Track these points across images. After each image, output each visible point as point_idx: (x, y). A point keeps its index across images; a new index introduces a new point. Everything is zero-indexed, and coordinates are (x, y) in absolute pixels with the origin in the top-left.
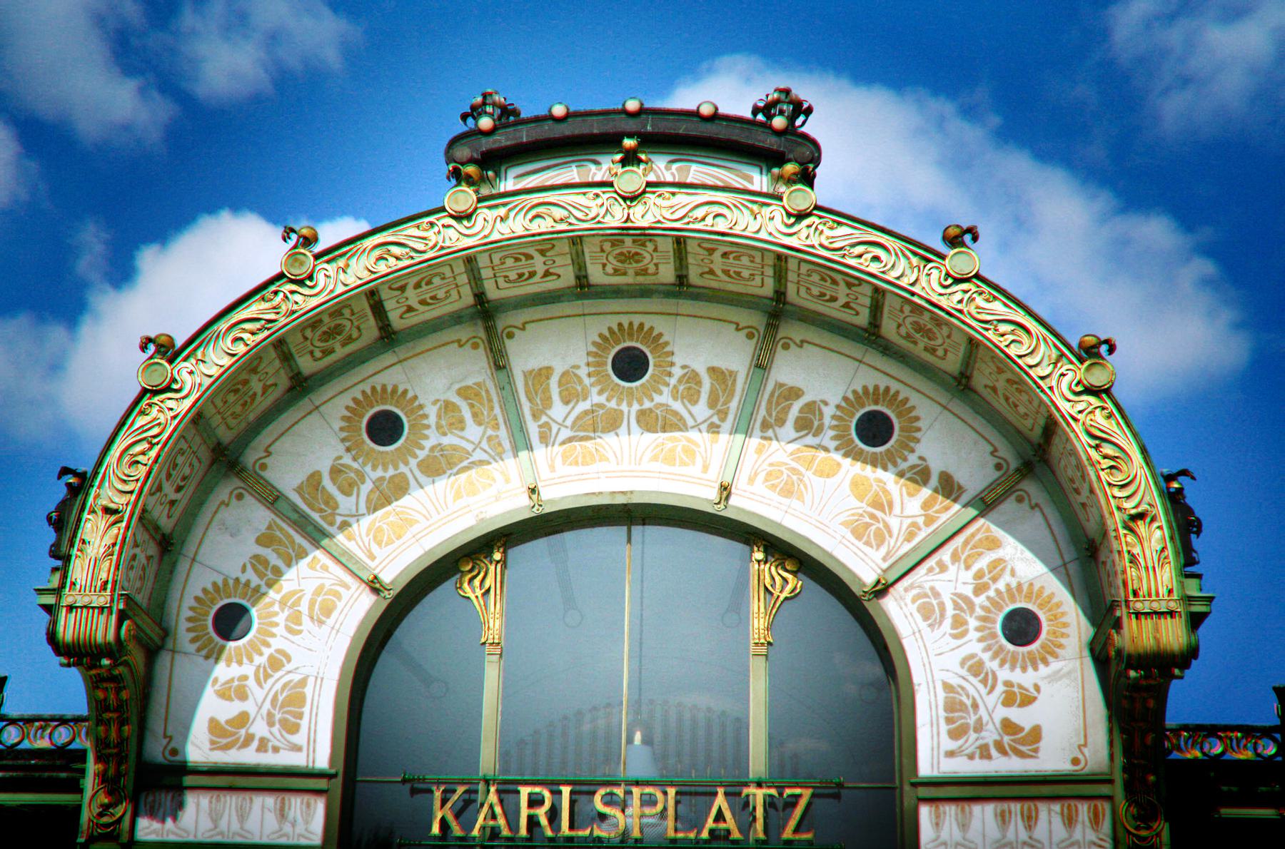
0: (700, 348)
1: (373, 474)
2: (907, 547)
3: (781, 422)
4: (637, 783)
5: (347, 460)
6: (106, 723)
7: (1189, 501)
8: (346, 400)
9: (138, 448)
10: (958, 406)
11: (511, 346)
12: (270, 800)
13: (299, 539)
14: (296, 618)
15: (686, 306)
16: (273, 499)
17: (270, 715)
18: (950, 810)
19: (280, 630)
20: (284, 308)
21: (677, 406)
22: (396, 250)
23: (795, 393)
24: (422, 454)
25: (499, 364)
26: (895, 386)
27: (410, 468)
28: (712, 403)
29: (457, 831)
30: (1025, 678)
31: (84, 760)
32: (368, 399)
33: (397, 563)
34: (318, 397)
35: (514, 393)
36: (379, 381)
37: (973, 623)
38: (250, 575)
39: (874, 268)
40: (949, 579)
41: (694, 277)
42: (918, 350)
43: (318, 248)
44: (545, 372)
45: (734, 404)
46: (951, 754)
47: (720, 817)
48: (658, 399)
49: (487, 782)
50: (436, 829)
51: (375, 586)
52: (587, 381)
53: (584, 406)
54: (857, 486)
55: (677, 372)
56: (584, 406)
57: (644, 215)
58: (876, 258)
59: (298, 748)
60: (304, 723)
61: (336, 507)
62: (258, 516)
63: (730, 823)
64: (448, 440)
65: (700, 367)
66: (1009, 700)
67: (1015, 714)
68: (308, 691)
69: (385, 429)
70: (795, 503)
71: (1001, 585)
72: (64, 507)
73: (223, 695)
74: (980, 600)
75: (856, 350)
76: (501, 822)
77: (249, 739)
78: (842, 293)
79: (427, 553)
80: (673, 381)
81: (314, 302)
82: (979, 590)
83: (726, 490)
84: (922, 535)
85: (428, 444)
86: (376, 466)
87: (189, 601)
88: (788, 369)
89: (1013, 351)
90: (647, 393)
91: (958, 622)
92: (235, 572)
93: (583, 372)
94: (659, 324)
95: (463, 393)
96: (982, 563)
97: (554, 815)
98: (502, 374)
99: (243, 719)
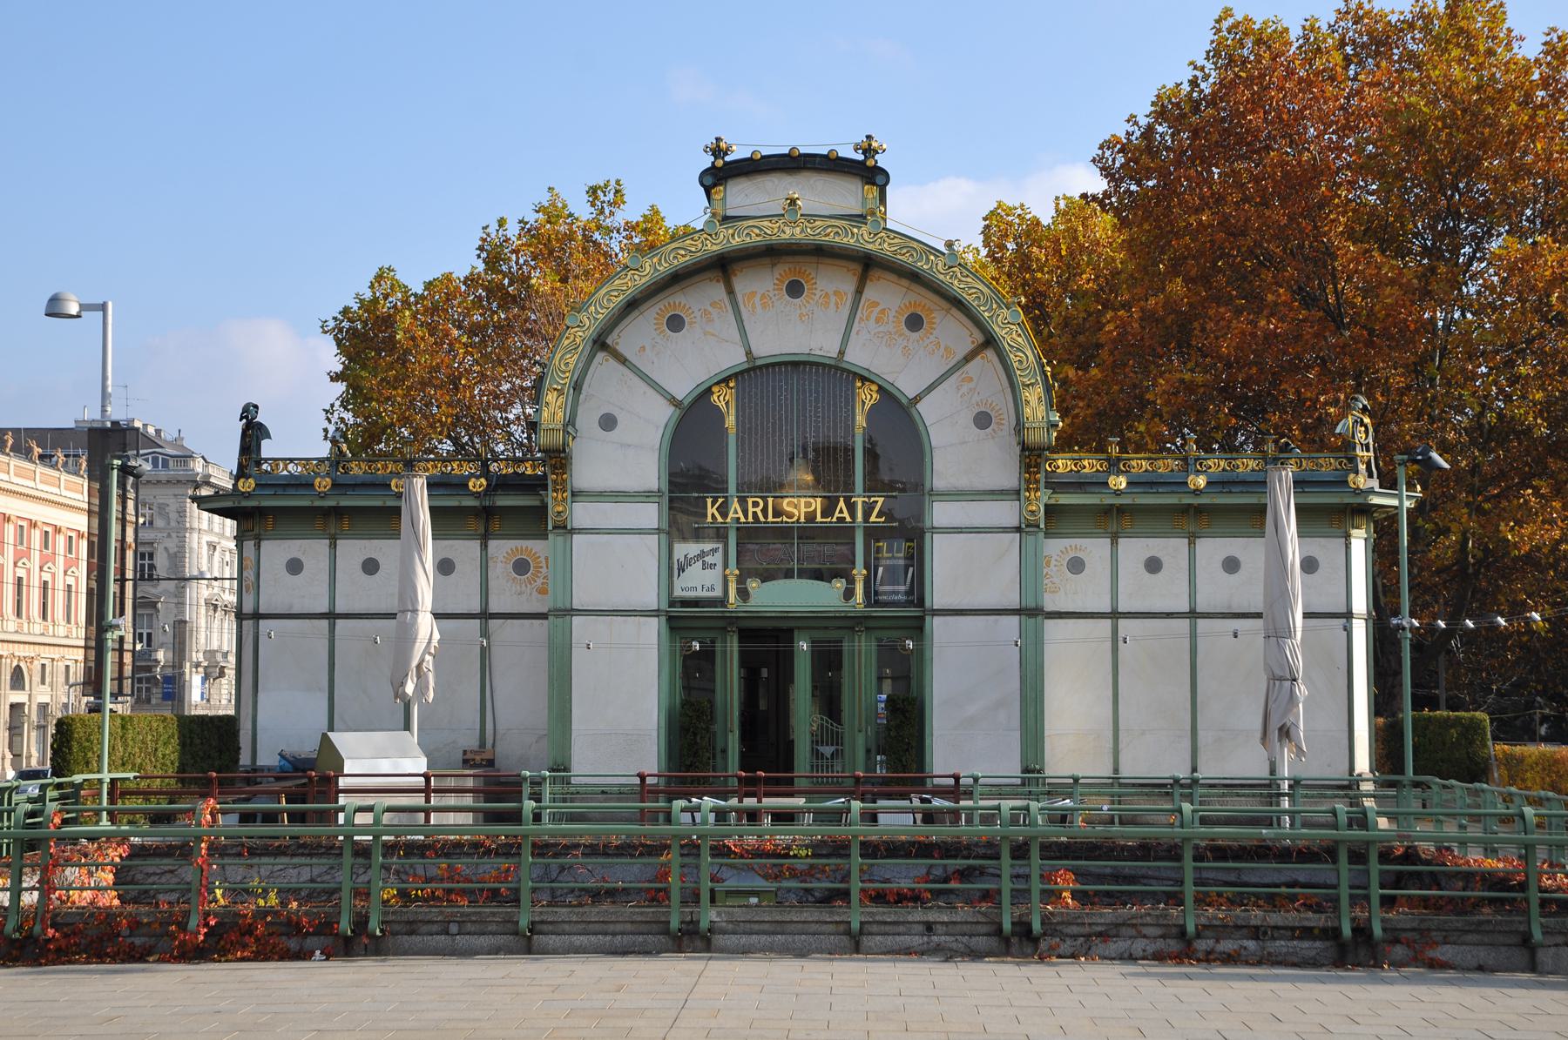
8: (656, 309)
10: (954, 311)
16: (623, 361)
33: (683, 389)
47: (841, 511)
50: (709, 519)
55: (818, 293)
63: (846, 514)
65: (831, 293)
76: (741, 515)
96: (964, 389)
97: (765, 511)
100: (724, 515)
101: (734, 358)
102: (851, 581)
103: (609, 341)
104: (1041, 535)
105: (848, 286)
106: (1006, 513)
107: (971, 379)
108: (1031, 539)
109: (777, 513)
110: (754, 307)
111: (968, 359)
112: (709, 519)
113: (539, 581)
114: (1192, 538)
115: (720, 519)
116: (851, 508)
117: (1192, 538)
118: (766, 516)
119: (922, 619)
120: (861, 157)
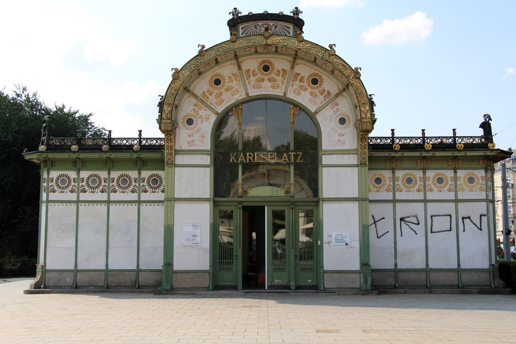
0: (280, 63)
1: (215, 91)
2: (321, 105)
3: (296, 80)
4: (269, 152)
5: (210, 89)
6: (168, 143)
7: (373, 100)
9: (173, 91)
10: (331, 77)
11: (242, 65)
12: (200, 156)
13: (202, 105)
14: (202, 121)
15: (277, 56)
16: (196, 96)
17: (199, 140)
18: (328, 156)
19: (199, 123)
20: (199, 62)
21: (275, 77)
22: (221, 50)
23: (299, 74)
24: (225, 87)
25: (240, 68)
26: (319, 73)
27: (223, 91)
28: (283, 76)
29: (235, 161)
30: (343, 132)
31: (164, 149)
32: (214, 76)
33: (220, 109)
34: (204, 76)
35: (243, 75)
36: (216, 72)
37: (333, 120)
38: (193, 113)
39: (315, 53)
41: (279, 50)
43: (205, 49)
44: (249, 70)
45: (287, 77)
46: (328, 146)
48: (272, 75)
49: (240, 152)
50: (231, 161)
51: (217, 113)
52: (257, 72)
53: (257, 77)
54: (311, 93)
55: (275, 70)
56: (257, 77)
57: (269, 41)
58: (315, 51)
59: (204, 146)
60: (205, 141)
61: (208, 98)
62: (193, 100)
63: (287, 159)
64: (230, 84)
66: (339, 135)
67: (340, 138)
68: (205, 135)
69: (217, 82)
70: (299, 97)
71: (338, 113)
72: (160, 103)
73: (190, 136)
74: (335, 116)
75: (311, 65)
76: (244, 159)
77: (195, 144)
78: (309, 56)
79: (227, 107)
80: (275, 72)
81: (205, 60)
82: (335, 114)
83: (285, 94)
84: (323, 103)
85: (226, 85)
86: (216, 90)
87: (181, 118)
88: (298, 69)
89: (341, 70)
90: (269, 74)
91: (330, 120)
92: (190, 112)
93: (257, 70)
94: (271, 60)
95: (233, 74)
98: (240, 71)
100: (237, 160)
101: (241, 96)
103: (191, 89)
104: (367, 168)
106: (353, 159)
107: (337, 105)
108: (363, 168)
110: (250, 76)
111: (337, 96)
112: (231, 161)
113: (162, 187)
114: (424, 170)
115: (235, 161)
116: (289, 156)
117: (424, 170)
118: (254, 160)
119: (318, 202)
120: (292, 15)
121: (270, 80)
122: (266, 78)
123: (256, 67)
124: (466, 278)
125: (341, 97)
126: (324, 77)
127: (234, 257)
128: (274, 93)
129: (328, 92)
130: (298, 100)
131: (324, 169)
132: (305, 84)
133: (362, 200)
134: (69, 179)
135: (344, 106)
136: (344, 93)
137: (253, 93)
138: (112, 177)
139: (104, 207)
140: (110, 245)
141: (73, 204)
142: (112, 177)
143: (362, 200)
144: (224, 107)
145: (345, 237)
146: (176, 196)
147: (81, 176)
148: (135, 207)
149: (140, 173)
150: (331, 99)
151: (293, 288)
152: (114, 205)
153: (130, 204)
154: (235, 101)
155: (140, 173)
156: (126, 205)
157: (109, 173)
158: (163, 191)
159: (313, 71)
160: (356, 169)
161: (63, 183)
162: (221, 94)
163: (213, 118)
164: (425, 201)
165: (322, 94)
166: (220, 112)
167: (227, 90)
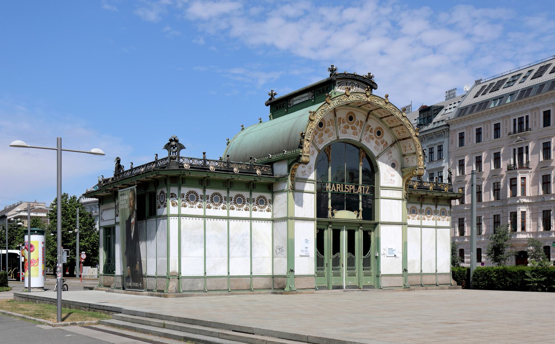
11: (337, 113)
15: (358, 110)
23: (370, 126)
25: (335, 116)
27: (323, 132)
33: (321, 147)
40: (385, 157)
42: (387, 123)
54: (376, 142)
64: (328, 128)
66: (391, 176)
67: (392, 178)
75: (378, 120)
88: (370, 122)
95: (331, 120)
99: (305, 171)
101: (333, 138)
102: (359, 211)
105: (363, 119)
107: (391, 153)
109: (344, 190)
111: (391, 146)
121: (352, 128)
122: (350, 126)
123: (345, 116)
124: (441, 280)
125: (393, 147)
126: (385, 131)
127: (325, 265)
128: (354, 139)
129: (386, 142)
130: (368, 146)
131: (382, 200)
132: (373, 134)
133: (403, 224)
134: (197, 195)
135: (395, 153)
136: (395, 144)
137: (342, 137)
138: (230, 196)
139: (225, 222)
140: (231, 256)
141: (201, 219)
142: (230, 196)
143: (403, 224)
144: (323, 146)
145: (394, 250)
146: (296, 216)
147: (207, 193)
148: (247, 223)
149: (251, 194)
150: (388, 148)
151: (362, 287)
152: (232, 220)
153: (244, 221)
154: (330, 141)
155: (251, 194)
156: (241, 221)
157: (228, 193)
158: (268, 211)
159: (379, 125)
160: (401, 201)
161: (192, 198)
162: (322, 135)
163: (316, 154)
164: (421, 227)
165: (382, 143)
166: (320, 149)
167: (326, 132)
